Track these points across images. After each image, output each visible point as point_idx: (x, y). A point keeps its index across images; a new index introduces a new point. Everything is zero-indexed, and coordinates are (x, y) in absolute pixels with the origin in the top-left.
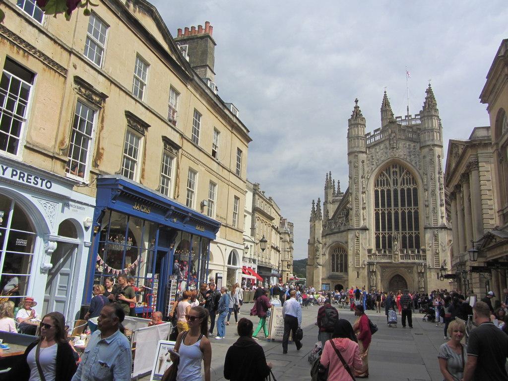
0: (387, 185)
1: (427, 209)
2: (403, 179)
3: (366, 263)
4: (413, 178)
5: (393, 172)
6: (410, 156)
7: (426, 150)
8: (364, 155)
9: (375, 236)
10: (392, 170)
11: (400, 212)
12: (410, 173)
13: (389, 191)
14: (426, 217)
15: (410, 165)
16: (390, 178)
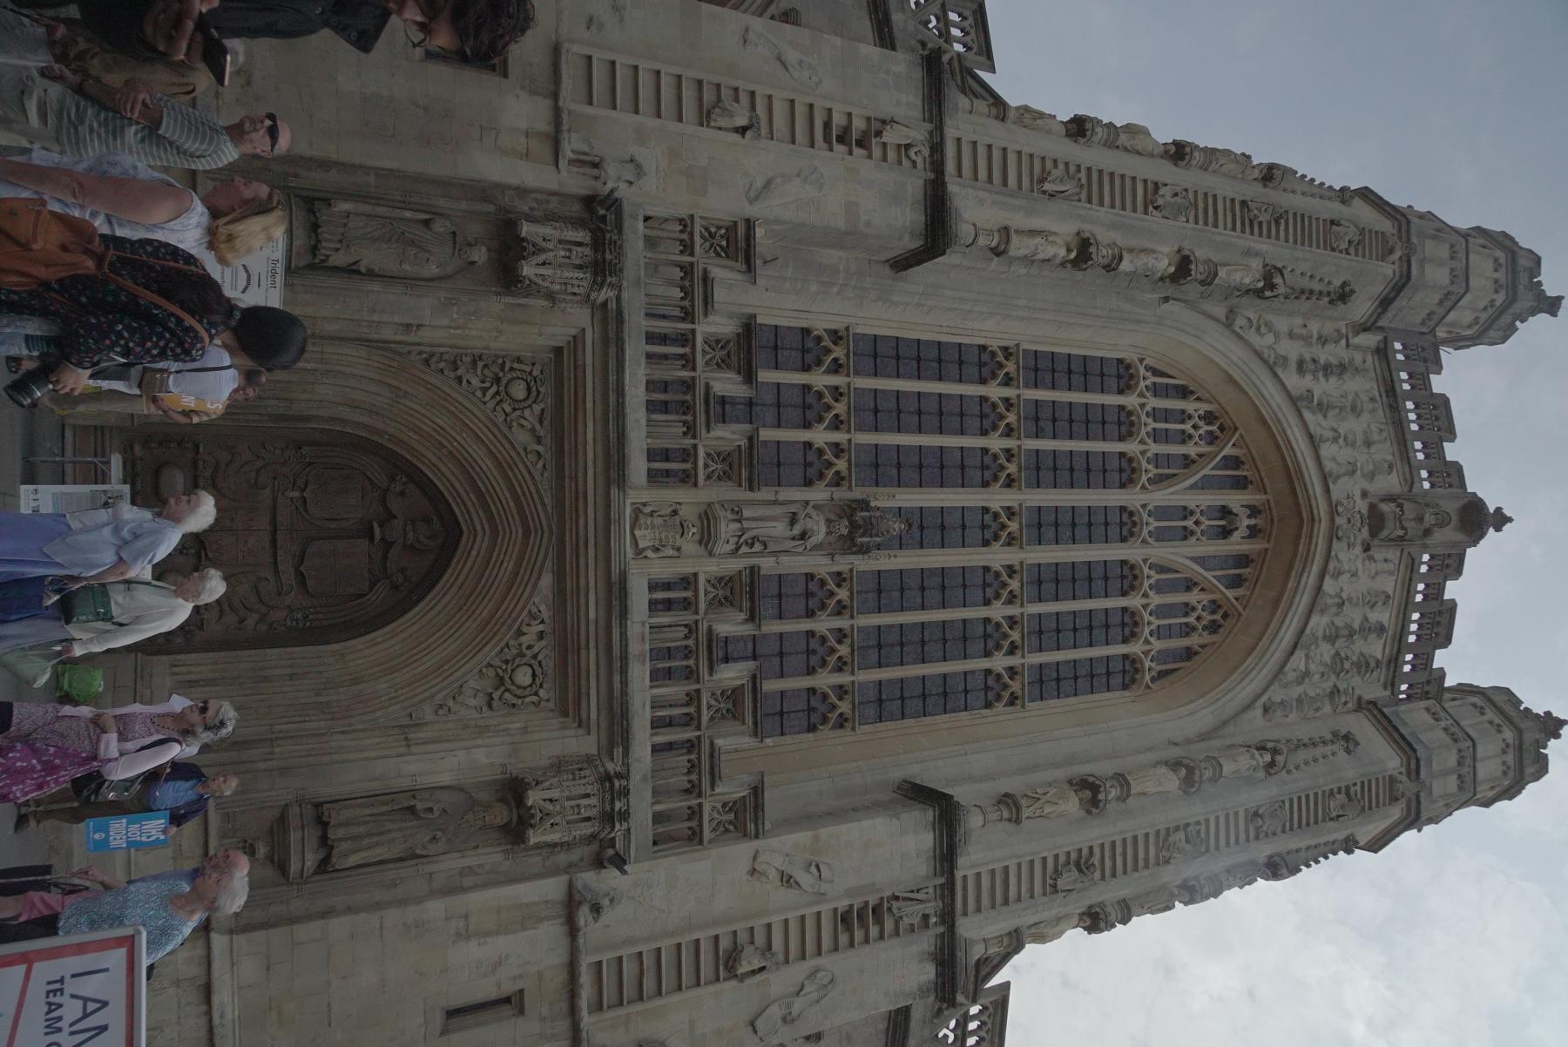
0: (1157, 460)
1: (1072, 804)
2: (1189, 585)
3: (614, 180)
4: (1189, 654)
5: (1225, 512)
6: (1331, 639)
7: (1393, 762)
8: (1361, 307)
9: (820, 325)
10: (1236, 500)
11: (997, 557)
12: (1213, 628)
13: (1126, 471)
14: (1009, 802)
15: (1287, 637)
16: (1192, 487)
